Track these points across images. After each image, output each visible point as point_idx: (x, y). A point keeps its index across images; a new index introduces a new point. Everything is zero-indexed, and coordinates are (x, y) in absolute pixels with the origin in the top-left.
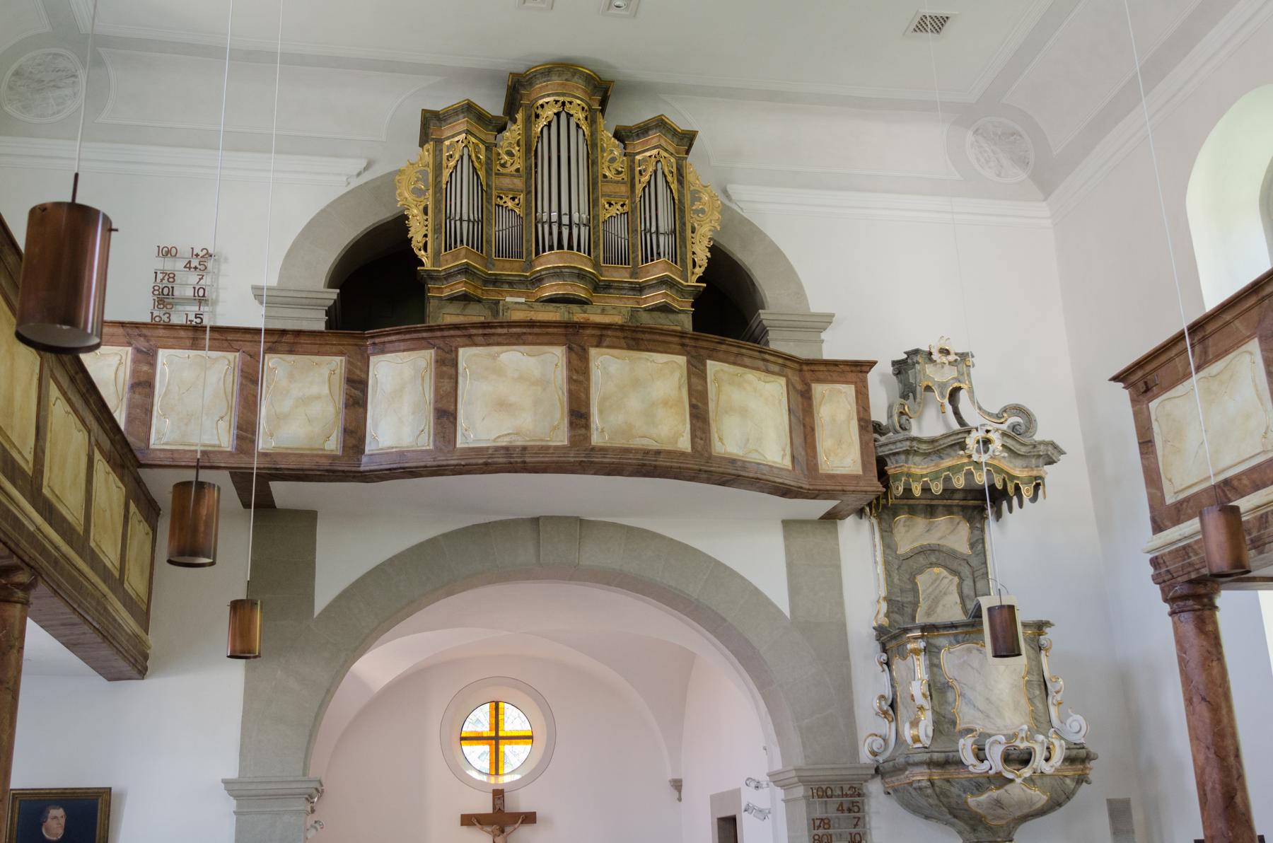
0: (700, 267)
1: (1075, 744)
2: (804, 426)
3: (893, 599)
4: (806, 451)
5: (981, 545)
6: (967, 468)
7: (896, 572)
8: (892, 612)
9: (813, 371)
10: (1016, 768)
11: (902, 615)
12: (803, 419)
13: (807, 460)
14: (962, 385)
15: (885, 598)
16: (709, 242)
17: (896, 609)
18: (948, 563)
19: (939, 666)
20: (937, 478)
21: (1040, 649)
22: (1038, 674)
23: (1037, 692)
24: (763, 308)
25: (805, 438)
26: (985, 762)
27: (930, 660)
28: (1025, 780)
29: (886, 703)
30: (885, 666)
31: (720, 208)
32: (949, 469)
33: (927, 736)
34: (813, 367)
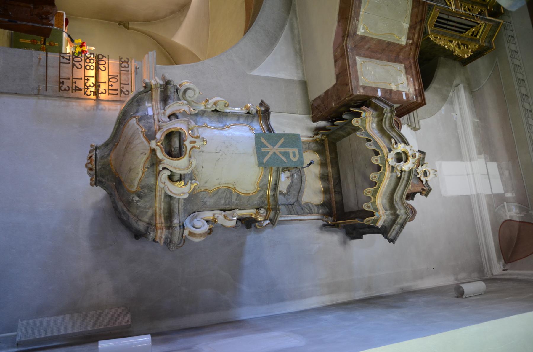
0: (435, 40)
9: (411, 66)
18: (294, 187)
21: (256, 209)
26: (168, 120)
28: (153, 151)
31: (463, 57)
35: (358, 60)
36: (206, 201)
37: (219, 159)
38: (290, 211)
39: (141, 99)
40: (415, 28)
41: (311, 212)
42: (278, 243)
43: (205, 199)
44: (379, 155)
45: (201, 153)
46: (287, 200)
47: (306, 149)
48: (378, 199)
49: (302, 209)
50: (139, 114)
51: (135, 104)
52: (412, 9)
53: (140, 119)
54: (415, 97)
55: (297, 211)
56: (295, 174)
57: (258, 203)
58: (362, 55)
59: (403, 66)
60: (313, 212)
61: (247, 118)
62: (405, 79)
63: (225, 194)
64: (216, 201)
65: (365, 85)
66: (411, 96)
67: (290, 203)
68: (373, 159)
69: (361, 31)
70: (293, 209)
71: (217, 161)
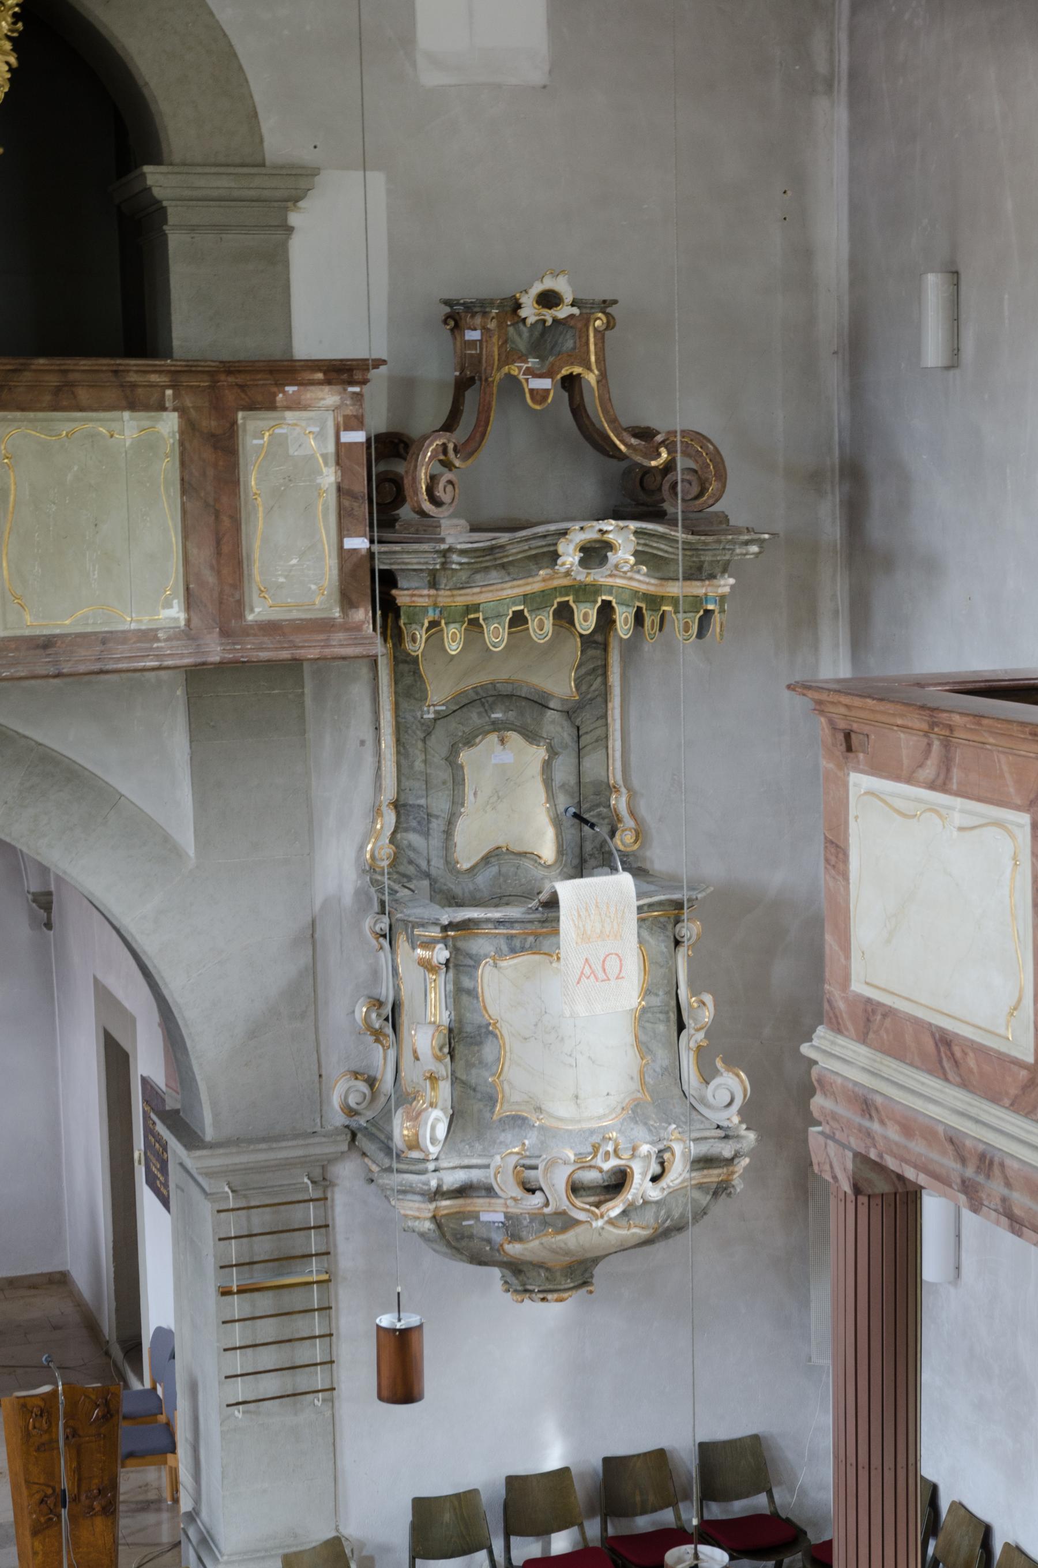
1: (718, 1127)
2: (217, 515)
3: (411, 802)
4: (219, 573)
5: (599, 680)
6: (559, 600)
7: (420, 744)
8: (406, 830)
10: (592, 1199)
11: (426, 834)
12: (217, 500)
13: (221, 593)
14: (577, 370)
15: (397, 805)
16: (15, 23)
17: (414, 824)
18: (529, 721)
19: (472, 993)
20: (499, 616)
21: (677, 943)
22: (667, 993)
23: (661, 1028)
24: (156, 159)
25: (218, 542)
26: (538, 1193)
27: (457, 983)
29: (379, 1015)
30: (386, 944)
32: (526, 598)
33: (433, 1140)
34: (240, 379)
35: (259, 613)
36: (661, 1067)
37: (589, 1057)
38: (597, 741)
39: (454, 1235)
40: (134, 386)
41: (600, 672)
42: (675, 777)
43: (658, 1069)
44: (571, 603)
45: (578, 1101)
46: (566, 747)
47: (414, 673)
48: (669, 589)
49: (592, 700)
50: (498, 1237)
51: (464, 1243)
52: (81, 409)
53: (515, 1237)
54: (351, 389)
55: (598, 719)
56: (493, 716)
57: (663, 941)
58: (237, 597)
59: (244, 418)
60: (599, 663)
61: (461, 968)
62: (289, 414)
63: (648, 1025)
64: (660, 1045)
65: (336, 596)
66: (348, 402)
67: (573, 738)
68: (582, 628)
69: (175, 613)
70: (591, 731)
71: (593, 1062)
